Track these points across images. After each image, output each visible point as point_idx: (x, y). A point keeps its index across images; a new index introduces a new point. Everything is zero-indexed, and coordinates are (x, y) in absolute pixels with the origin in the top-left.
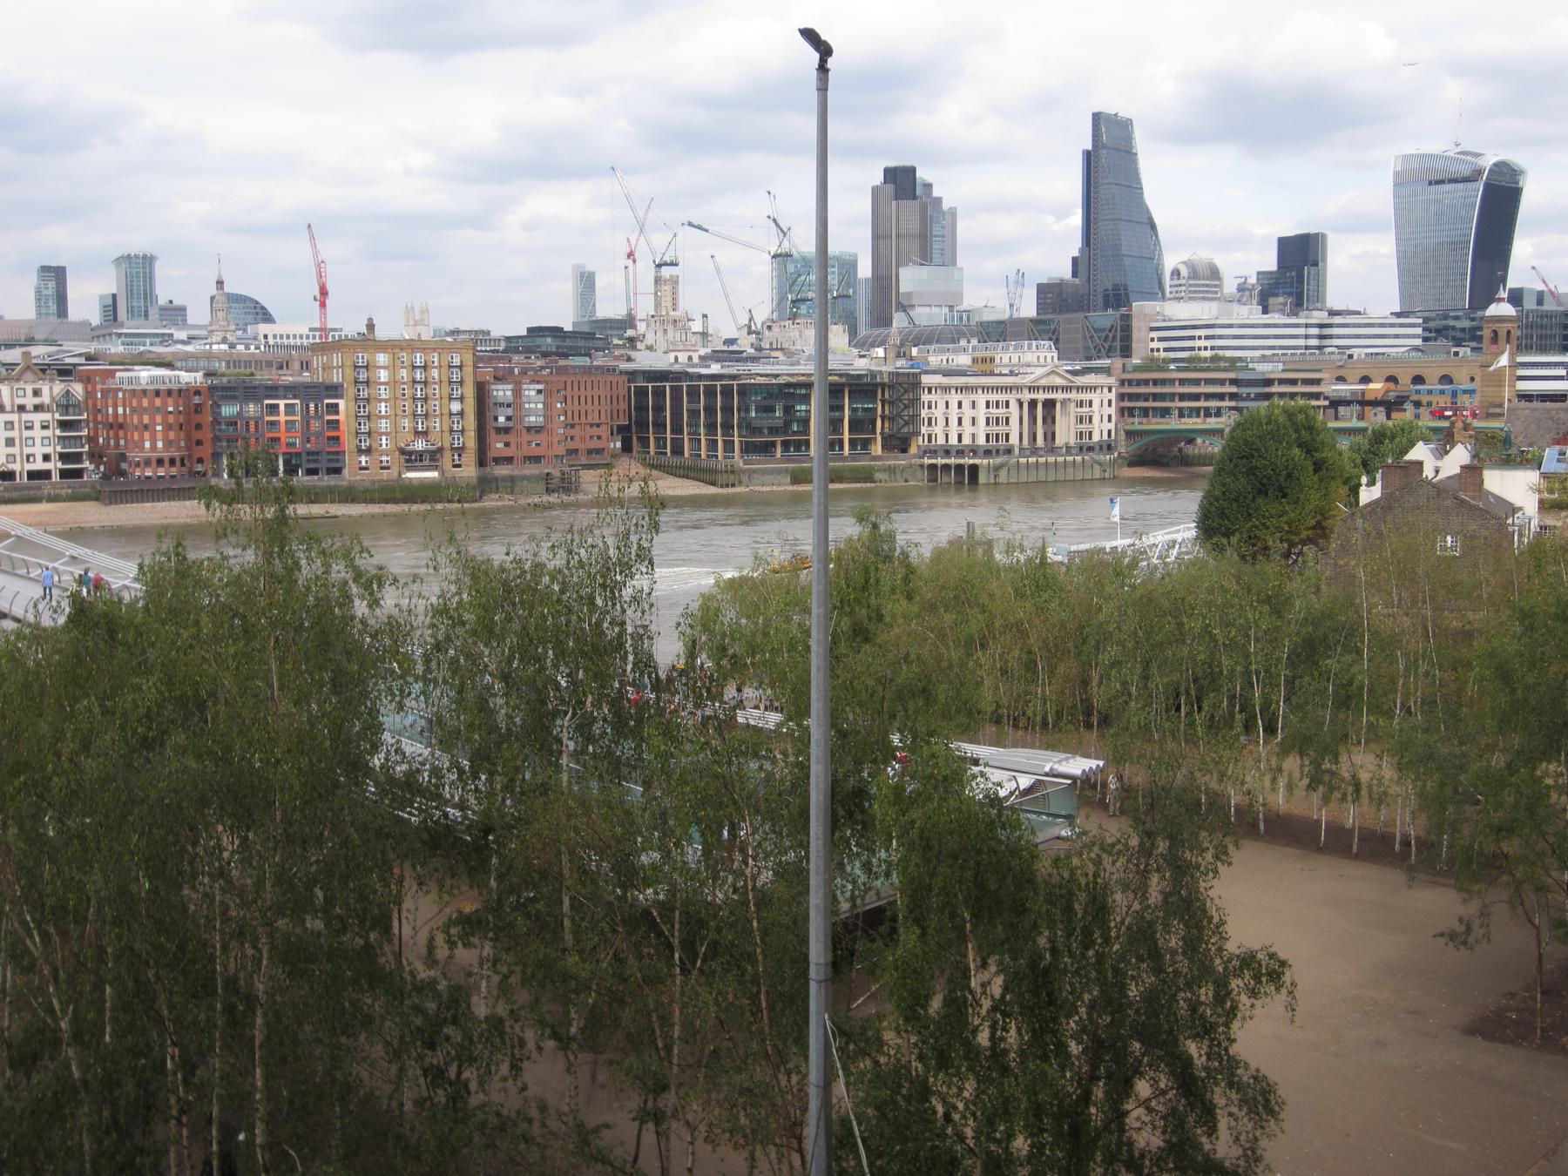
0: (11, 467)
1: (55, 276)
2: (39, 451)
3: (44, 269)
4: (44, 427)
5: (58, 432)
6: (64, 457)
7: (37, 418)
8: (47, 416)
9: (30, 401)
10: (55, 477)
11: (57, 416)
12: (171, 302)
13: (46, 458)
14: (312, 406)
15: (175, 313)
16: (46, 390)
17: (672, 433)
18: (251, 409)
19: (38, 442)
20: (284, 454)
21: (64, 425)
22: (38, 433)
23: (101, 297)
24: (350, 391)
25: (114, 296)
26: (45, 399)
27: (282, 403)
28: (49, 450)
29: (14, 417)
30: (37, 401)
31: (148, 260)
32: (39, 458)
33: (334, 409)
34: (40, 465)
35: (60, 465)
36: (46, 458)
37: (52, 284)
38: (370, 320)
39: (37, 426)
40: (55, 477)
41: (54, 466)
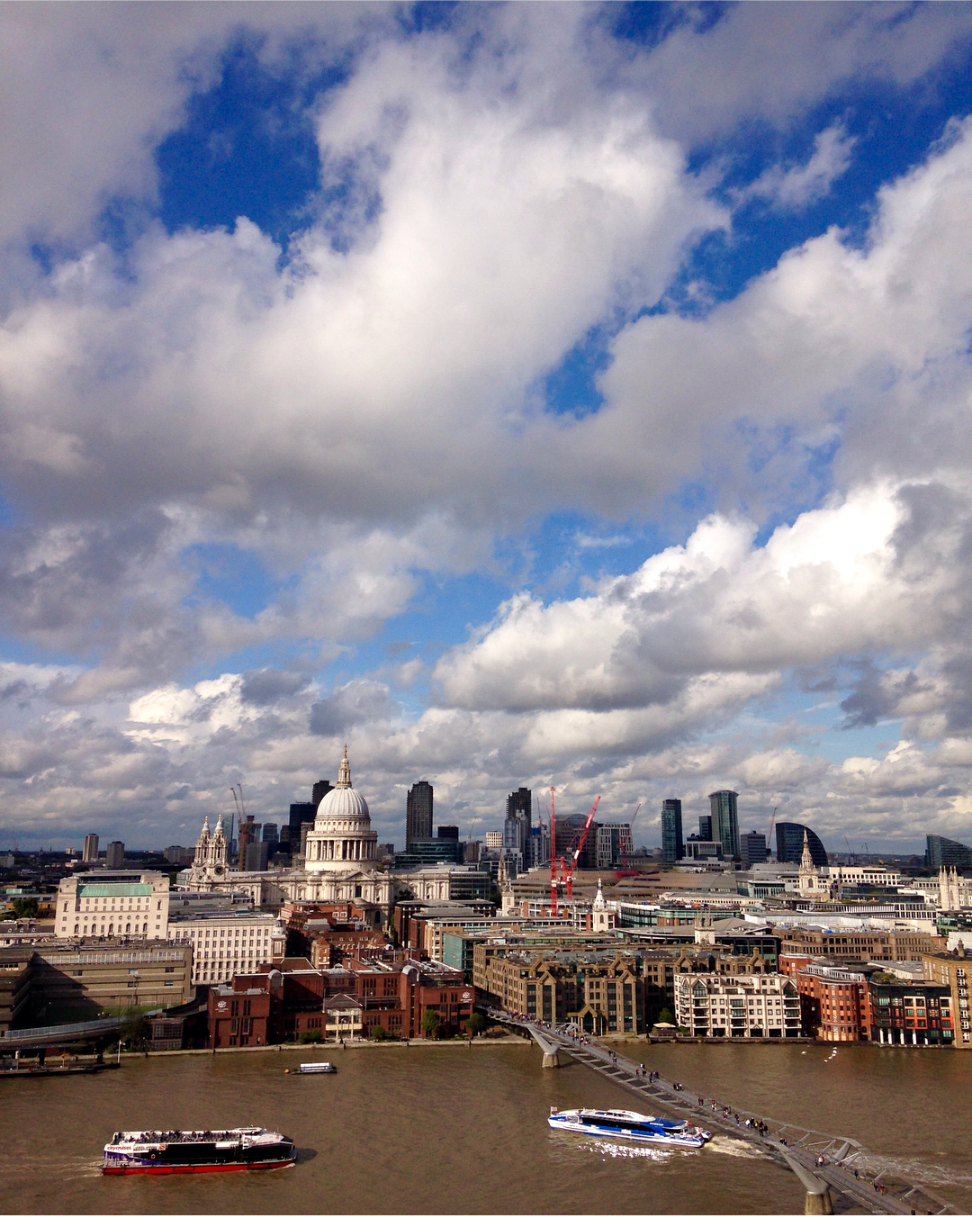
0: (761, 1026)
1: (674, 806)
2: (775, 1017)
4: (777, 1004)
5: (784, 1007)
6: (788, 1022)
7: (774, 998)
8: (778, 997)
9: (768, 987)
10: (783, 1034)
11: (784, 997)
12: (755, 832)
14: (932, 1000)
15: (756, 839)
16: (777, 981)
18: (897, 1001)
19: (774, 1012)
20: (917, 1031)
21: (786, 1002)
22: (774, 1007)
24: (954, 991)
25: (709, 818)
26: (777, 987)
27: (914, 998)
28: (780, 1017)
29: (762, 997)
30: (772, 987)
32: (775, 1022)
33: (945, 1003)
34: (775, 1027)
35: (786, 1026)
37: (673, 813)
38: (960, 941)
39: (774, 1003)
40: (783, 1034)
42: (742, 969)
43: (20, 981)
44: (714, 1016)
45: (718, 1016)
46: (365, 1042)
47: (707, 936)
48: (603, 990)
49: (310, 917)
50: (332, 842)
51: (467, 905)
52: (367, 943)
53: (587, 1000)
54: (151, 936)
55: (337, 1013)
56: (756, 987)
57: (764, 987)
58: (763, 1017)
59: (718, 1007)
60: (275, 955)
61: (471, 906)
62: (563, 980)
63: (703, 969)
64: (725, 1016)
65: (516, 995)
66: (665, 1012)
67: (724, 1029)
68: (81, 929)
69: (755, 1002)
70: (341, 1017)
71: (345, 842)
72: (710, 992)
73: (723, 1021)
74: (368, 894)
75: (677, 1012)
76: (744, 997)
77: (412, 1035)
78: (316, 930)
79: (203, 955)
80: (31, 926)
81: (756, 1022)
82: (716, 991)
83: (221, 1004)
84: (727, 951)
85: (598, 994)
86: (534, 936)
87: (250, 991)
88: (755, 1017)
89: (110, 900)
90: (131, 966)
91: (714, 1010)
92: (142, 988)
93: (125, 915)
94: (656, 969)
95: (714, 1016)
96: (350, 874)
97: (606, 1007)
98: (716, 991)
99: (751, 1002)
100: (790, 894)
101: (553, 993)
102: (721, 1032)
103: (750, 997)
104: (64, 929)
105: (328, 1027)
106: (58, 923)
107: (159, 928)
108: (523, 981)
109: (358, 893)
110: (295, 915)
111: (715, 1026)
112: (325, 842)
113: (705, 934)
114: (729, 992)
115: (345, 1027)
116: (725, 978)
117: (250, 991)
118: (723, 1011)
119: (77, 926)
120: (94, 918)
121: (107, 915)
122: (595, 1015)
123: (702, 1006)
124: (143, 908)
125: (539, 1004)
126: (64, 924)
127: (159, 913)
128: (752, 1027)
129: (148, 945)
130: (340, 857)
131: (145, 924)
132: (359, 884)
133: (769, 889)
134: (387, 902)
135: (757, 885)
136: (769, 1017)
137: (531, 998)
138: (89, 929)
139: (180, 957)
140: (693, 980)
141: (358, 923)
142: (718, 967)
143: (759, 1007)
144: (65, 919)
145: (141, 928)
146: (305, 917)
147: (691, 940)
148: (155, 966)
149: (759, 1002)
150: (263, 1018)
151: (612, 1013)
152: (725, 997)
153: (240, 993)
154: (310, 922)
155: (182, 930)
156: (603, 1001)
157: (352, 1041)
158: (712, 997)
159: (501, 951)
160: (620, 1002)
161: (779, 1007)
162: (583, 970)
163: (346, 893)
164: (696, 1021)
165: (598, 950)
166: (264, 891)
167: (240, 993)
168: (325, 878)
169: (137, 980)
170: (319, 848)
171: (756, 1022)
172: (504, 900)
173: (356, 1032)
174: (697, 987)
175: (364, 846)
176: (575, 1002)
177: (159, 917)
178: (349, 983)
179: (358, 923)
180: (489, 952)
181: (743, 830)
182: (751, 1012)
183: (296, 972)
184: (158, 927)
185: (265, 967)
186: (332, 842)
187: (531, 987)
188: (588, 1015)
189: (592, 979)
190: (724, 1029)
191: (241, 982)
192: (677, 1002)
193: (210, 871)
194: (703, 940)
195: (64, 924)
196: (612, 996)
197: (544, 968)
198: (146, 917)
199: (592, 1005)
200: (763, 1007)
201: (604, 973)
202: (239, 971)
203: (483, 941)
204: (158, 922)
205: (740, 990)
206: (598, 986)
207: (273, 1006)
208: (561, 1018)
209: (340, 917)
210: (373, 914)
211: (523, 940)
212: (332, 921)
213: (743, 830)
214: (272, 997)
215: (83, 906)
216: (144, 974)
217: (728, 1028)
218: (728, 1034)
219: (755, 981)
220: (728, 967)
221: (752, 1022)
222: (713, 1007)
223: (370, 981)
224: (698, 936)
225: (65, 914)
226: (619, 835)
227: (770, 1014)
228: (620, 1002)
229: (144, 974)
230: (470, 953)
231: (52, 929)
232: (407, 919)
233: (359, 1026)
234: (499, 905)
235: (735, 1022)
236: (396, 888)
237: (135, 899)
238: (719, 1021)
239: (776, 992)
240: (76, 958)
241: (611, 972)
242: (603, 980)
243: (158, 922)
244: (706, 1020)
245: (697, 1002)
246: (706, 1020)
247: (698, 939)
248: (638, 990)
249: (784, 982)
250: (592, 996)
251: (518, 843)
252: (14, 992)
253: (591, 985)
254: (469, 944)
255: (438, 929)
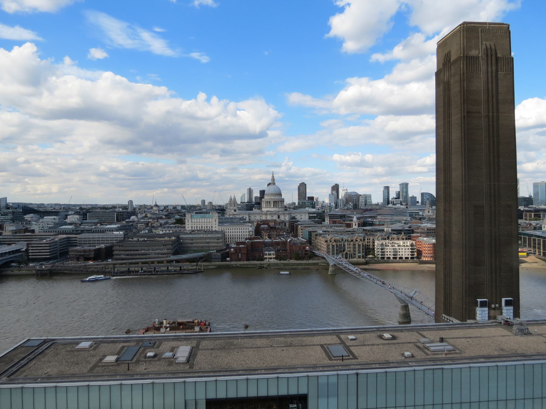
0: (402, 256)
1: (387, 188)
2: (407, 253)
3: (385, 187)
5: (410, 250)
6: (411, 255)
7: (407, 248)
8: (408, 247)
9: (405, 244)
10: (410, 258)
11: (410, 247)
13: (408, 255)
15: (414, 198)
16: (408, 243)
17: (543, 250)
21: (411, 249)
22: (407, 250)
23: (396, 192)
25: (399, 192)
26: (408, 244)
29: (403, 247)
30: (407, 244)
31: (407, 185)
34: (407, 256)
35: (410, 256)
36: (408, 255)
37: (386, 190)
39: (407, 249)
40: (410, 258)
41: (410, 256)
42: (398, 239)
43: (174, 242)
44: (387, 253)
45: (389, 253)
46: (276, 261)
47: (388, 229)
48: (352, 246)
49: (263, 224)
50: (270, 202)
51: (312, 221)
52: (280, 232)
53: (346, 249)
54: (214, 230)
55: (267, 253)
56: (401, 244)
57: (404, 244)
58: (403, 253)
59: (388, 251)
60: (250, 235)
61: (313, 221)
62: (339, 243)
63: (385, 239)
64: (391, 253)
65: (324, 247)
66: (372, 252)
67: (390, 257)
68: (193, 227)
69: (401, 249)
70: (269, 254)
71: (274, 202)
72: (386, 246)
73: (390, 255)
74: (282, 218)
75: (375, 252)
76: (397, 248)
77: (291, 259)
78: (263, 229)
79: (227, 235)
80: (179, 227)
81: (401, 255)
82: (388, 246)
83: (232, 249)
84: (394, 234)
85: (350, 247)
86: (332, 230)
87: (241, 246)
88: (401, 253)
89: (201, 219)
90: (206, 238)
91: (387, 252)
92: (210, 245)
93: (206, 224)
94: (370, 239)
95: (387, 253)
96: (276, 212)
97: (353, 251)
98: (388, 246)
99: (399, 249)
100: (420, 215)
101: (335, 247)
102: (389, 258)
103: (399, 248)
104: (188, 227)
105: (265, 257)
106: (186, 226)
107: (216, 227)
108: (326, 243)
109: (279, 217)
110: (258, 224)
111: (387, 256)
112: (268, 202)
113: (387, 229)
114: (392, 246)
115: (270, 256)
116: (391, 242)
117: (241, 246)
118: (390, 252)
119: (192, 227)
120: (197, 224)
121: (201, 224)
122: (348, 253)
123: (383, 251)
124: (211, 222)
125: (331, 250)
126: (188, 226)
127: (216, 223)
128: (399, 256)
129: (212, 232)
130: (273, 207)
131: (212, 226)
132: (279, 215)
133: (414, 214)
134: (288, 220)
135: (410, 213)
136: (405, 253)
137: (328, 248)
138: (196, 227)
139: (221, 236)
140: (381, 243)
141: (277, 226)
142: (390, 239)
143: (402, 250)
144: (188, 224)
145: (211, 227)
146: (260, 225)
147: (383, 230)
148: (213, 238)
149: (402, 249)
150: (245, 254)
151: (354, 253)
152: (391, 247)
153: (238, 246)
154: (262, 226)
155: (223, 228)
156: (352, 249)
157: (272, 261)
158: (387, 247)
159: (320, 235)
160: (357, 249)
161: (408, 250)
162: (346, 240)
163: (275, 217)
164: (381, 255)
165: (351, 234)
166: (249, 216)
167: (238, 246)
168: (268, 213)
169: (208, 243)
170: (266, 204)
171: (401, 255)
172: (326, 219)
173: (273, 258)
174: (382, 245)
175: (280, 203)
176: (343, 250)
177: (216, 224)
178: (272, 244)
179: (277, 226)
180: (316, 235)
181: (410, 195)
182: (399, 252)
183: (256, 240)
184: (216, 227)
185: (246, 239)
186: (270, 202)
187: (328, 246)
188: (347, 253)
189: (348, 243)
190: (390, 257)
191: (238, 243)
192: (375, 249)
193: (233, 211)
194: (387, 230)
195: (188, 226)
196: (354, 248)
197: (333, 240)
198: (212, 224)
199: (348, 251)
200: (403, 250)
201: (352, 241)
202: (236, 240)
203: (314, 232)
204: (216, 226)
205: (396, 245)
206: (350, 244)
207: (248, 250)
208: (337, 254)
209: (272, 224)
210: (284, 224)
211: (328, 231)
212: (269, 226)
213: (410, 195)
214: (247, 248)
215: (193, 221)
216: (211, 241)
217: (392, 257)
218: (392, 258)
219: (401, 242)
220: (394, 238)
221: (399, 255)
222: (387, 251)
223: (278, 244)
224: (386, 229)
225: (188, 223)
226: (367, 197)
227: (405, 252)
228: (357, 249)
229: (211, 241)
230: (311, 235)
231: (185, 227)
232: (293, 225)
233: (274, 256)
234: (324, 221)
235: (394, 255)
236: (291, 216)
237: (208, 219)
238: (389, 255)
239: (407, 246)
240: (191, 236)
241: (354, 241)
242: (352, 243)
243: (216, 226)
244: (385, 254)
245: (382, 249)
246: (385, 254)
247: (385, 230)
248: (363, 246)
249: (411, 243)
250: (348, 248)
251: (333, 202)
252: (172, 245)
253: (348, 244)
254: (310, 233)
255: (302, 228)
